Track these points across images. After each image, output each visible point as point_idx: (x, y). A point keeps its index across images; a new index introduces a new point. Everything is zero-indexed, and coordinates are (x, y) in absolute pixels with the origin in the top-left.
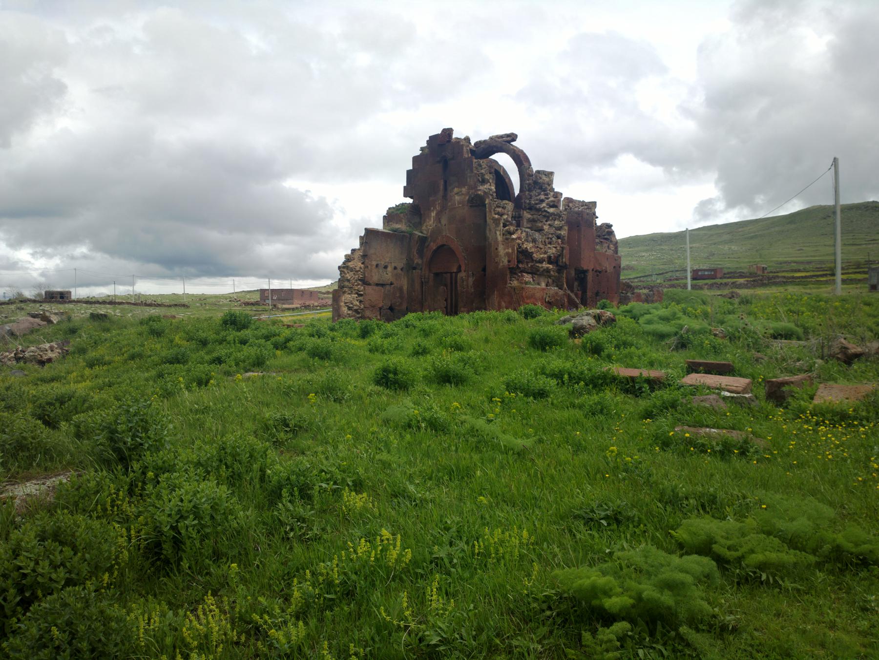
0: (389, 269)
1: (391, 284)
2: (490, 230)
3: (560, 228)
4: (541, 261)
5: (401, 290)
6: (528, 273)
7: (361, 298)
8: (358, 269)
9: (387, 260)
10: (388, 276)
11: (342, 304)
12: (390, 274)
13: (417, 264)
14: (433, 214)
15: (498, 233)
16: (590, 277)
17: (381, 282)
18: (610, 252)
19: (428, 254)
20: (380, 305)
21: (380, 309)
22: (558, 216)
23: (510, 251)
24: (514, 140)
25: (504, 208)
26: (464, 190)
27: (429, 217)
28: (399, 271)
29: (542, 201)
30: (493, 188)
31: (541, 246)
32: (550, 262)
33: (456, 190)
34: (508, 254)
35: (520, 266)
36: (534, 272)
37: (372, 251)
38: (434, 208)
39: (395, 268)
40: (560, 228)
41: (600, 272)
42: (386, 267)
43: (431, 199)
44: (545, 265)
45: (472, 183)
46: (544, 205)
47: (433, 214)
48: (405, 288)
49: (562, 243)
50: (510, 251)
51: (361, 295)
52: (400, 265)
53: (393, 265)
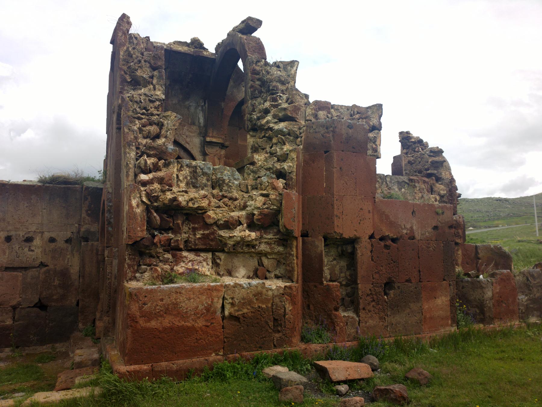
0: (37, 242)
1: (42, 265)
3: (283, 158)
4: (229, 225)
5: (64, 274)
6: (196, 251)
9: (33, 228)
10: (36, 252)
12: (38, 251)
13: (88, 231)
16: (363, 252)
17: (16, 265)
18: (432, 199)
20: (14, 303)
21: (14, 308)
22: (293, 136)
24: (255, 30)
25: (161, 125)
28: (61, 244)
29: (266, 112)
30: (160, 94)
31: (235, 194)
32: (251, 226)
35: (160, 237)
36: (213, 247)
40: (283, 158)
41: (394, 240)
42: (29, 240)
44: (241, 233)
46: (269, 118)
48: (75, 269)
49: (287, 186)
52: (62, 235)
53: (47, 235)
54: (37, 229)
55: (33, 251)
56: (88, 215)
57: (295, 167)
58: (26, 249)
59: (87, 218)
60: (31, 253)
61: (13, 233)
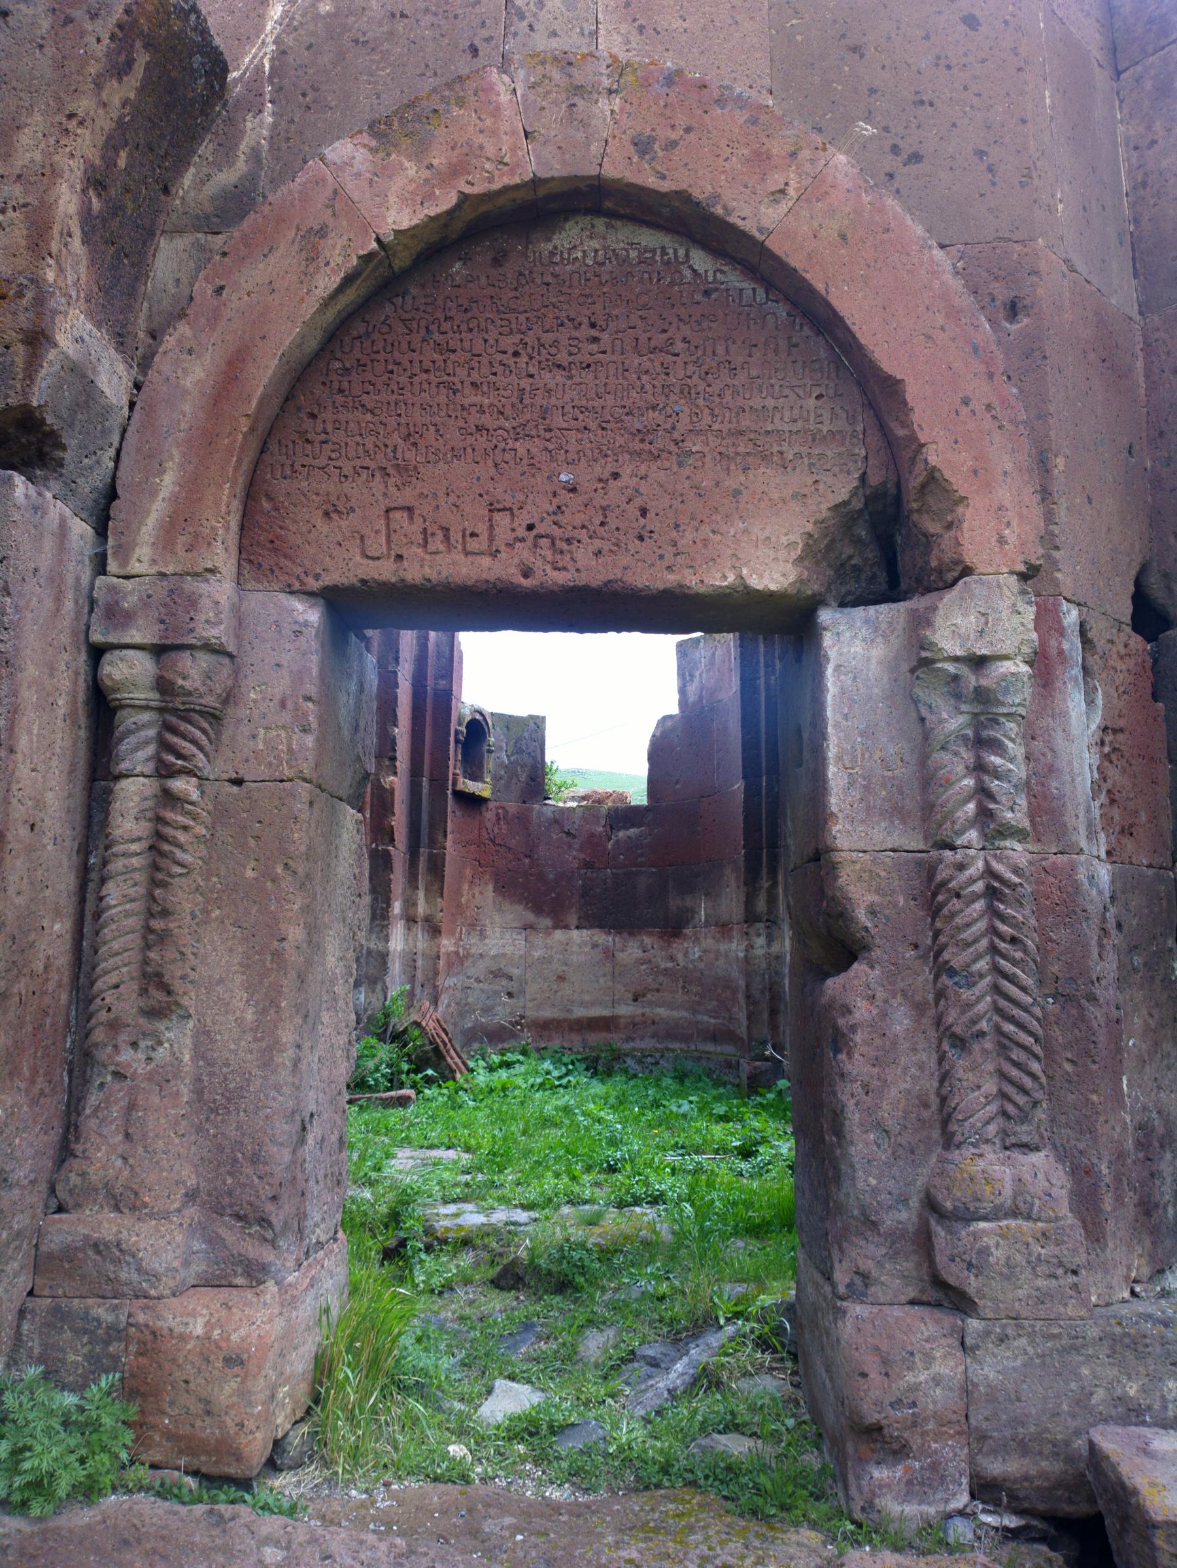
19: (285, 294)
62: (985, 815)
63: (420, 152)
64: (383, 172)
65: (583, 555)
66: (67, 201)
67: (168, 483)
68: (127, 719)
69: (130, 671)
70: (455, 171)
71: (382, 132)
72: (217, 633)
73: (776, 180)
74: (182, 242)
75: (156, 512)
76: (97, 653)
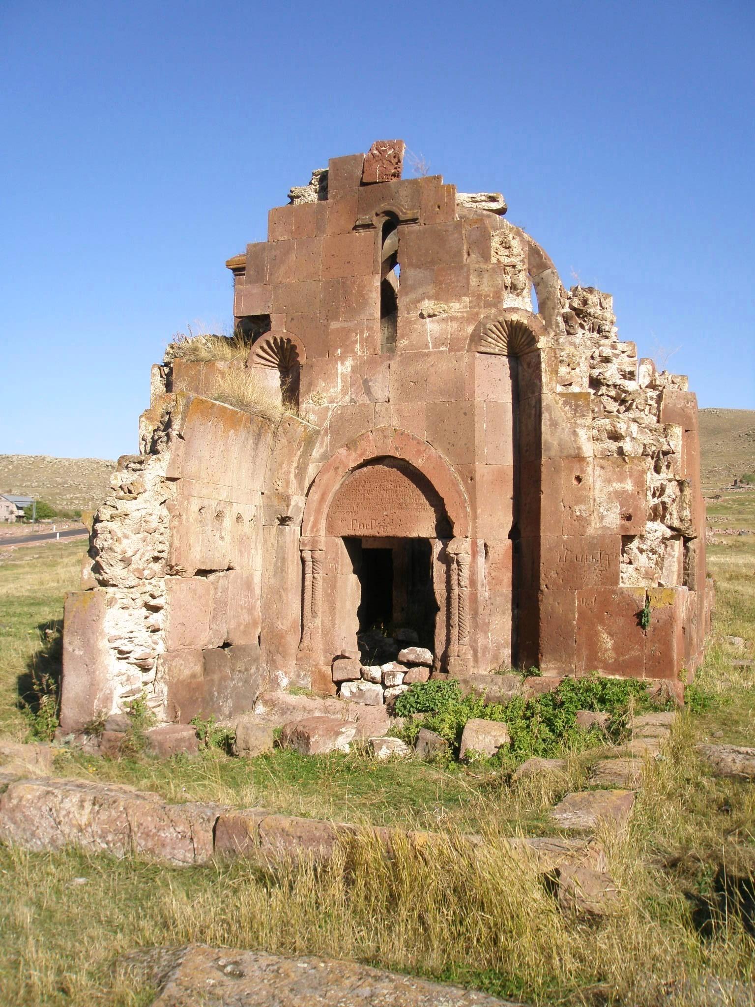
0: (228, 522)
2: (554, 424)
5: (248, 585)
7: (156, 619)
8: (154, 523)
9: (223, 497)
11: (103, 644)
12: (228, 538)
14: (345, 368)
15: (583, 434)
23: (629, 486)
26: (456, 307)
27: (329, 377)
33: (427, 306)
34: (621, 496)
37: (192, 467)
38: (348, 350)
39: (239, 518)
42: (219, 516)
43: (334, 325)
45: (486, 288)
47: (345, 368)
48: (257, 579)
50: (629, 486)
51: (156, 609)
53: (236, 509)
54: (227, 496)
55: (222, 538)
56: (296, 476)
57: (680, 446)
58: (218, 535)
59: (294, 481)
60: (220, 542)
61: (206, 503)
62: (459, 584)
63: (355, 451)
64: (349, 455)
65: (389, 529)
66: (292, 476)
67: (312, 519)
68: (307, 563)
69: (307, 555)
70: (362, 454)
71: (348, 447)
72: (323, 548)
73: (422, 456)
74: (314, 465)
75: (310, 524)
76: (301, 551)
